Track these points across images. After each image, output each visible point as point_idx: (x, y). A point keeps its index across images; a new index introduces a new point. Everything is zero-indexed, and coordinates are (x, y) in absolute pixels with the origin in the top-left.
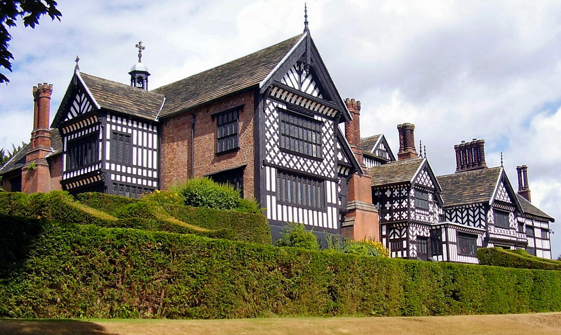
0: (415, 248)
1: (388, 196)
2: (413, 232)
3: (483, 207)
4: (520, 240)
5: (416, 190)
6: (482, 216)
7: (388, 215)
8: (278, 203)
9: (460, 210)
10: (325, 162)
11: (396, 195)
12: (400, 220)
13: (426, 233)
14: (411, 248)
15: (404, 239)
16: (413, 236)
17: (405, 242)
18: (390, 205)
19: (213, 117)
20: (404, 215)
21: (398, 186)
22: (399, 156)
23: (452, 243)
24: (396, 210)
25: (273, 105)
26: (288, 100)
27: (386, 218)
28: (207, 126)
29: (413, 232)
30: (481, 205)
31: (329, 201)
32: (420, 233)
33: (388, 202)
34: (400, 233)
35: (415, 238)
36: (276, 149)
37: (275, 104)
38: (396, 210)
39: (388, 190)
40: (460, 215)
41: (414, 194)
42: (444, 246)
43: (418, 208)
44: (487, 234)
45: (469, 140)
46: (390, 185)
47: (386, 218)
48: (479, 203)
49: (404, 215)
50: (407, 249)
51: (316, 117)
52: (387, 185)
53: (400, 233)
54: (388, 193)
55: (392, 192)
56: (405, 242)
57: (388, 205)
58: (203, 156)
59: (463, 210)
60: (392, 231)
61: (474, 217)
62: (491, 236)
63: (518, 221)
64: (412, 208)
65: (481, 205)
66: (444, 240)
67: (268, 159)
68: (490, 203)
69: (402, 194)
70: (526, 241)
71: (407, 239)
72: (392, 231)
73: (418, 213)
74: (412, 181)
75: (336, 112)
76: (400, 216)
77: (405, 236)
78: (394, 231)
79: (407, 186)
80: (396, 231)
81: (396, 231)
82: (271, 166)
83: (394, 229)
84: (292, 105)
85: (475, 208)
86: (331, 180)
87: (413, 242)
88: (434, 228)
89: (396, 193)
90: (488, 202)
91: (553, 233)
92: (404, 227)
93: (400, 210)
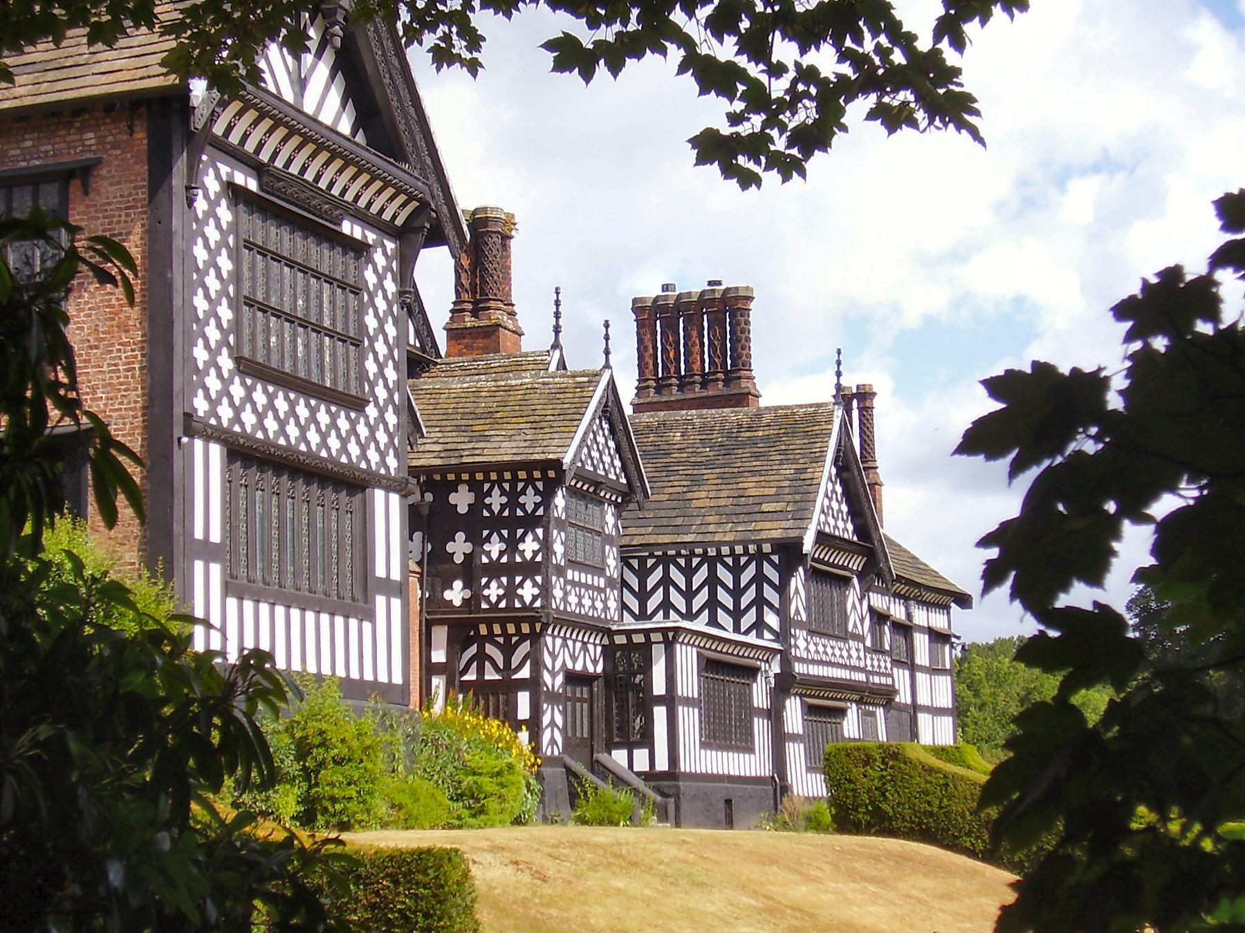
0: (559, 720)
1: (463, 509)
2: (554, 657)
3: (775, 558)
4: (876, 680)
5: (573, 492)
6: (770, 594)
7: (458, 584)
9: (682, 562)
10: (371, 411)
11: (496, 509)
12: (510, 607)
13: (590, 660)
14: (546, 720)
15: (523, 684)
16: (553, 675)
17: (523, 699)
18: (468, 548)
20: (528, 591)
21: (507, 475)
22: (454, 334)
23: (688, 702)
24: (494, 570)
25: (218, 176)
26: (264, 157)
27: (448, 595)
29: (554, 657)
30: (767, 548)
31: (380, 572)
32: (574, 659)
33: (460, 536)
34: (507, 661)
35: (560, 679)
36: (226, 363)
37: (224, 169)
38: (494, 570)
39: (463, 489)
40: (680, 580)
41: (566, 508)
42: (660, 713)
43: (573, 564)
44: (787, 662)
45: (693, 284)
46: (472, 468)
47: (448, 595)
48: (759, 543)
50: (534, 725)
51: (346, 227)
52: (459, 469)
53: (507, 661)
54: (462, 500)
55: (481, 495)
56: (523, 699)
57: (459, 547)
59: (695, 561)
60: (473, 649)
61: (737, 593)
63: (871, 609)
64: (558, 566)
65: (767, 548)
66: (659, 688)
67: (201, 405)
69: (523, 507)
70: (889, 681)
71: (533, 685)
72: (473, 649)
73: (574, 584)
74: (567, 460)
75: (415, 204)
76: (511, 592)
77: (525, 673)
78: (481, 649)
79: (544, 478)
80: (490, 649)
81: (490, 649)
83: (482, 641)
84: (279, 176)
85: (743, 560)
87: (554, 698)
88: (620, 640)
89: (496, 500)
90: (799, 543)
92: (523, 638)
93: (511, 570)
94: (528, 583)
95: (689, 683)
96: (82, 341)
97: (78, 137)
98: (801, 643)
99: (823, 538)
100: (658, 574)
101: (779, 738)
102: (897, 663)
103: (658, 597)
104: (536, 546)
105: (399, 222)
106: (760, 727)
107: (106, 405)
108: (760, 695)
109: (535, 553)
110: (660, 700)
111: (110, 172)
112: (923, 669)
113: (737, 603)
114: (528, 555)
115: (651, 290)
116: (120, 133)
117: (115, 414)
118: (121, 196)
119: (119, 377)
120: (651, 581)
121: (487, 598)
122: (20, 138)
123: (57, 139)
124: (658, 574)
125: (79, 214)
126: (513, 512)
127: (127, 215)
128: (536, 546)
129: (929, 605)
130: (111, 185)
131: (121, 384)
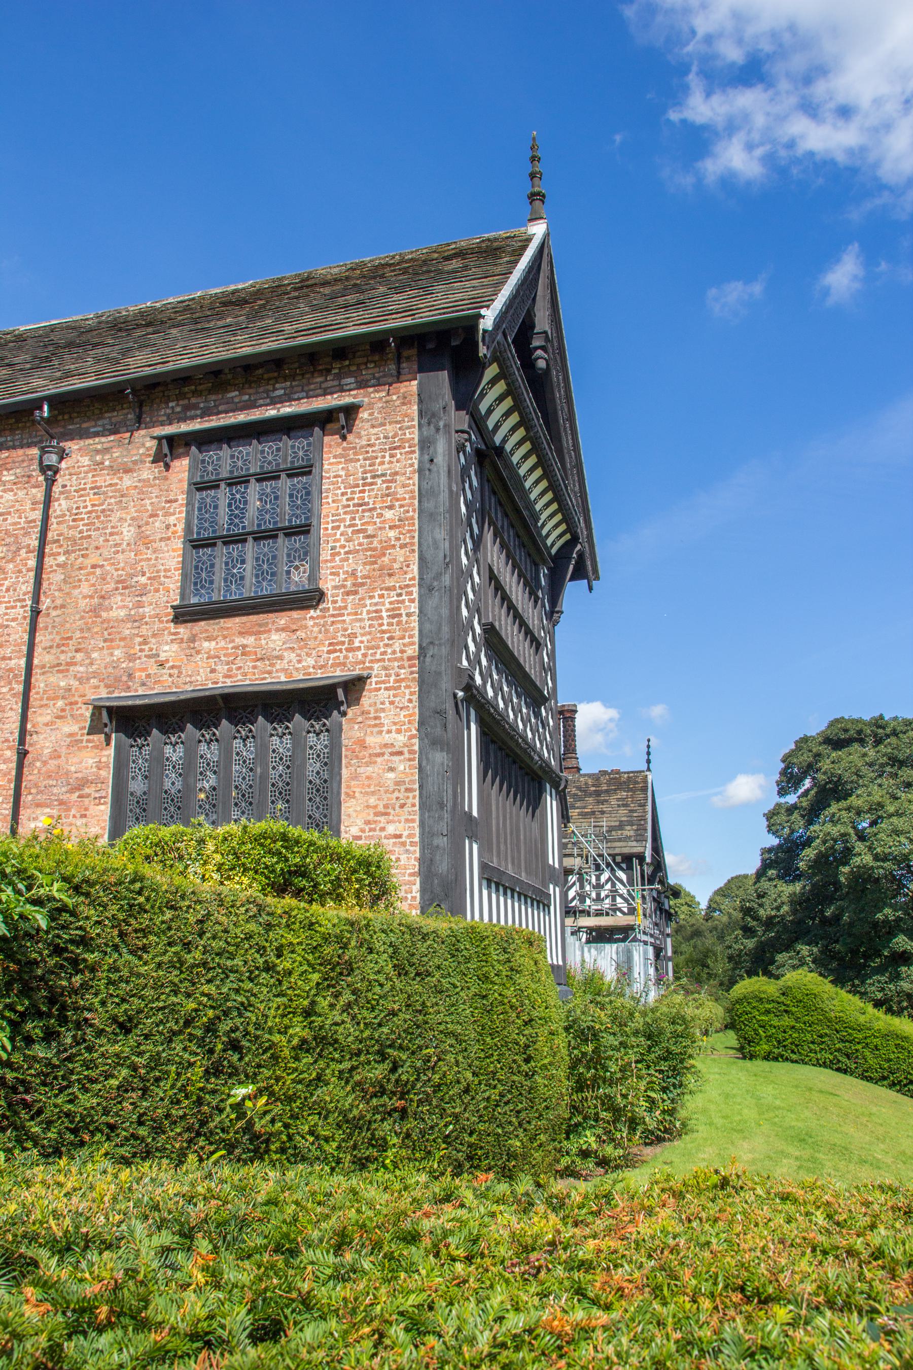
28: (127, 481)
30: (619, 859)
58: (95, 611)
96: (335, 587)
97: (336, 383)
107: (365, 655)
111: (371, 414)
116: (384, 376)
117: (376, 666)
118: (385, 437)
119: (382, 625)
122: (271, 388)
123: (312, 387)
125: (335, 457)
127: (392, 456)
130: (373, 427)
131: (384, 632)
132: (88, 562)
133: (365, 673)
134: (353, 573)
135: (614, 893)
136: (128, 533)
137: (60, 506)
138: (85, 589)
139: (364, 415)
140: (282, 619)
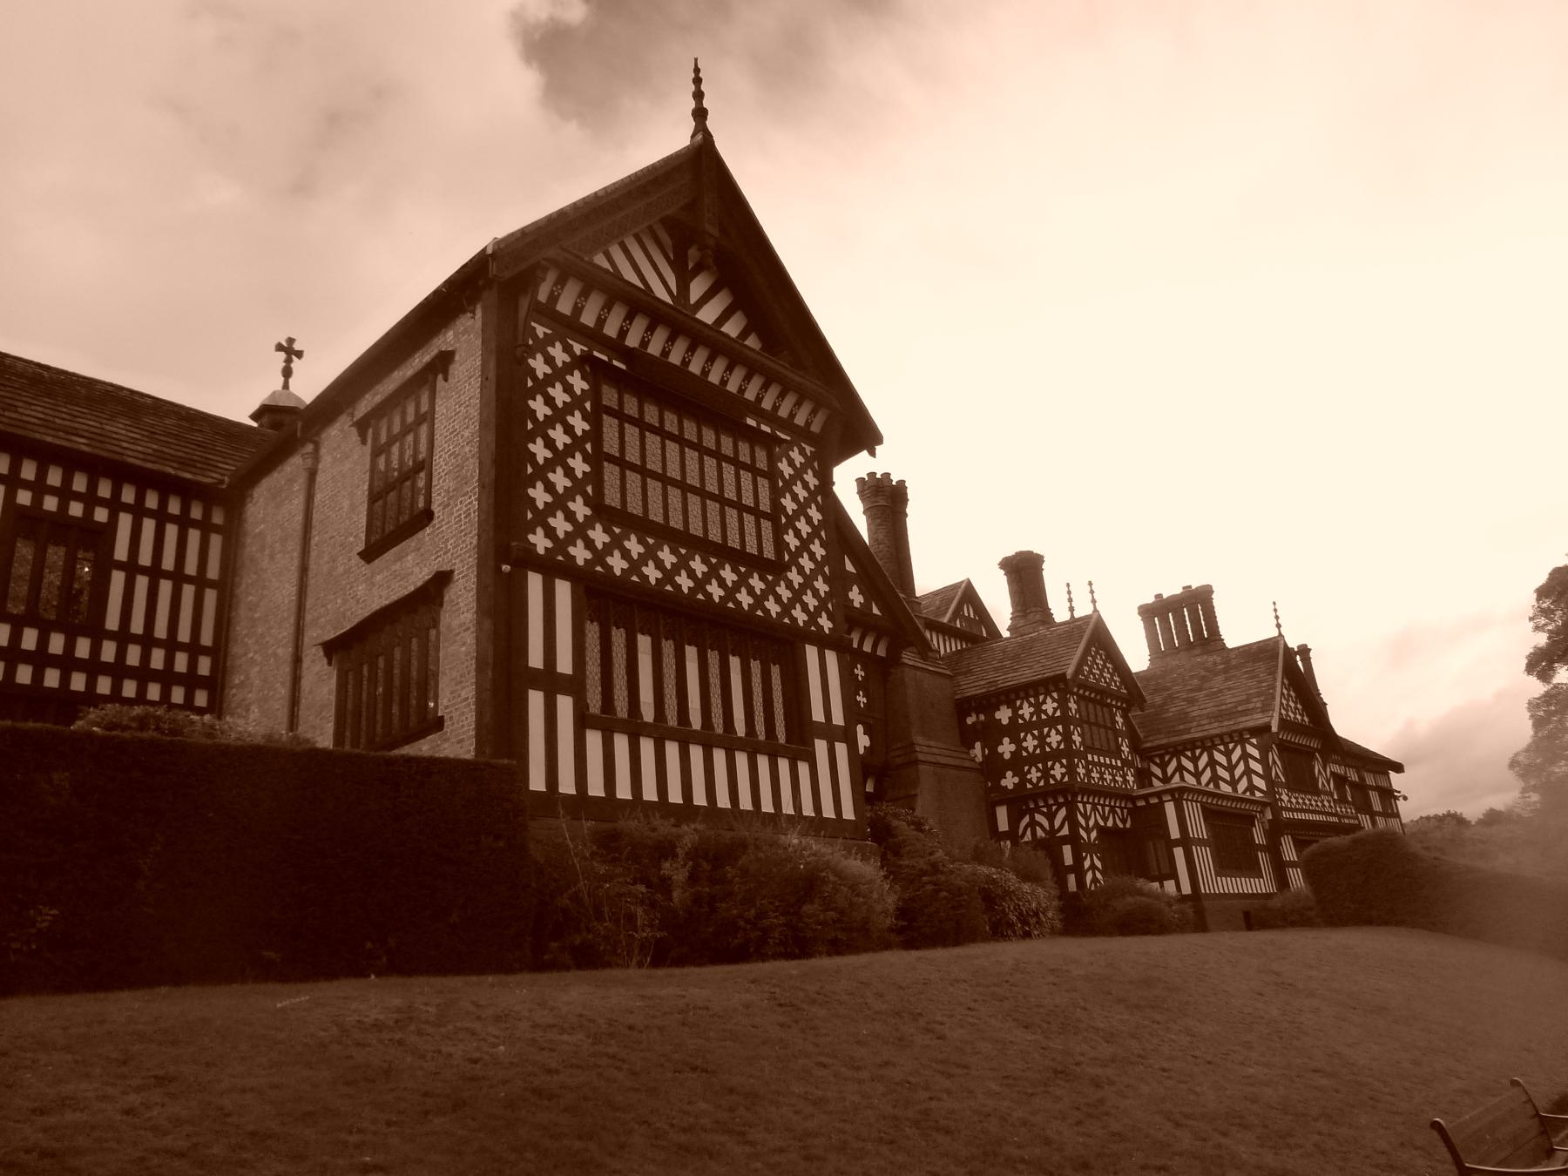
0: (1098, 864)
1: (1005, 722)
2: (1087, 819)
5: (1081, 699)
7: (1009, 774)
8: (583, 722)
10: (795, 577)
11: (1027, 717)
14: (1087, 864)
17: (1067, 851)
18: (1013, 747)
19: (362, 426)
20: (1058, 771)
23: (1200, 842)
25: (567, 349)
26: (632, 341)
27: (1003, 783)
29: (1087, 819)
31: (818, 715)
32: (1105, 819)
33: (1006, 740)
35: (1094, 835)
36: (579, 508)
37: (578, 348)
38: (1032, 760)
40: (1190, 766)
41: (1078, 711)
42: (1179, 852)
44: (1277, 812)
45: (1172, 589)
47: (1003, 783)
49: (1058, 771)
50: (1078, 868)
51: (751, 422)
54: (1004, 715)
55: (1015, 710)
56: (1067, 851)
57: (1006, 748)
60: (1026, 819)
61: (1231, 768)
62: (1286, 815)
66: (1175, 833)
67: (540, 541)
68: (1274, 729)
71: (1073, 839)
72: (1026, 819)
73: (1093, 763)
74: (1070, 672)
77: (1065, 831)
78: (1032, 818)
80: (1038, 817)
81: (1038, 817)
82: (553, 568)
83: (1031, 812)
86: (823, 642)
87: (1091, 848)
88: (1141, 803)
90: (1267, 727)
91: (1405, 798)
92: (1060, 806)
93: (1044, 757)
94: (1057, 765)
95: (1198, 828)
98: (1285, 798)
99: (1285, 724)
100: (1174, 764)
101: (1280, 867)
102: (1359, 810)
103: (1177, 778)
104: (1059, 738)
105: (816, 428)
106: (1263, 859)
108: (1259, 837)
109: (1059, 743)
110: (1177, 843)
112: (1380, 814)
113: (1232, 775)
114: (1054, 745)
115: (1150, 599)
120: (1170, 770)
121: (1030, 781)
124: (1174, 764)
126: (1039, 717)
128: (1059, 738)
129: (1374, 772)
132: (327, 536)
133: (446, 568)
134: (447, 491)
135: (1248, 772)
136: (346, 504)
137: (318, 497)
138: (326, 558)
139: (457, 358)
140: (411, 543)
